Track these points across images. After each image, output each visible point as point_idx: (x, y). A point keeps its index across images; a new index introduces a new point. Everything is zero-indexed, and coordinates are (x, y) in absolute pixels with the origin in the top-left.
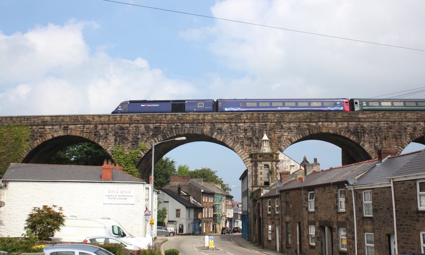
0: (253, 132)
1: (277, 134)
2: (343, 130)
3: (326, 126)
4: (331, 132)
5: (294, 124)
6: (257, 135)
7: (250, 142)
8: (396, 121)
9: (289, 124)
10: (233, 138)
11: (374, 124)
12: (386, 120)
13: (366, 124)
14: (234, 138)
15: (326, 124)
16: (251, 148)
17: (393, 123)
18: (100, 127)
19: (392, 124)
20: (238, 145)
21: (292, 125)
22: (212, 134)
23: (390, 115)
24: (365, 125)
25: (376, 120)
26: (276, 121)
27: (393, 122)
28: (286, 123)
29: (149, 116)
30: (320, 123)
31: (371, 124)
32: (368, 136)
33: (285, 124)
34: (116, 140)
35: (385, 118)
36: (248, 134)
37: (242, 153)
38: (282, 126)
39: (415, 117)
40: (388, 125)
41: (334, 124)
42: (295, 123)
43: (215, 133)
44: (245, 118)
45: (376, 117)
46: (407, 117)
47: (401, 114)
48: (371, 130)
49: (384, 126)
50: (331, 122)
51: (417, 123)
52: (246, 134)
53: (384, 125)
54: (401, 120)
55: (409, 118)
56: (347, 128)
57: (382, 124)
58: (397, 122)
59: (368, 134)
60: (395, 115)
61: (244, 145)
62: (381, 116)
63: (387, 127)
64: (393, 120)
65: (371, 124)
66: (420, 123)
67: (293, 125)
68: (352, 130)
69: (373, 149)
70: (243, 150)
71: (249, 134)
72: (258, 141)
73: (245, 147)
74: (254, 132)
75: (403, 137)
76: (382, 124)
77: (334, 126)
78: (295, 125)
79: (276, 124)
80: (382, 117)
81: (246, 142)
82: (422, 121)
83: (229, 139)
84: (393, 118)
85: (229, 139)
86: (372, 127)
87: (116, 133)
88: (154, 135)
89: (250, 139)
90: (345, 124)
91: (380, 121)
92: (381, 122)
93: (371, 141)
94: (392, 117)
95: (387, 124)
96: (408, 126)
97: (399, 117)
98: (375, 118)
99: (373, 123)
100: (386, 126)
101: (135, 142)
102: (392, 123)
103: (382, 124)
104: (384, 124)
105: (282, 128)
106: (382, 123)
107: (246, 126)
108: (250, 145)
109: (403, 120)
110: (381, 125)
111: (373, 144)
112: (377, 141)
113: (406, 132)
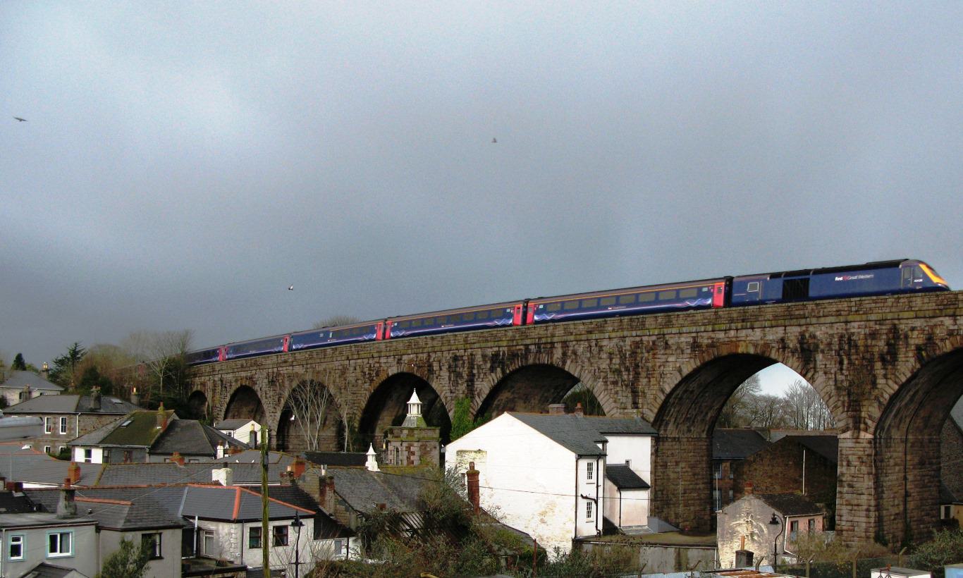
0: (621, 357)
1: (660, 360)
2: (773, 347)
3: (743, 339)
4: (752, 351)
5: (687, 338)
6: (628, 364)
7: (616, 376)
8: (886, 320)
9: (679, 338)
10: (593, 371)
11: (839, 328)
12: (864, 317)
13: (821, 330)
14: (595, 370)
15: (743, 333)
16: (618, 389)
17: (880, 324)
18: (433, 355)
19: (878, 327)
20: (599, 384)
21: (683, 339)
22: (564, 363)
23: (873, 305)
24: (818, 333)
25: (842, 319)
26: (656, 332)
27: (878, 323)
28: (673, 336)
29: (486, 335)
30: (732, 333)
31: (832, 327)
32: (823, 357)
33: (671, 338)
34: (450, 379)
35: (861, 312)
36: (614, 361)
37: (605, 400)
38: (666, 343)
39: (930, 308)
40: (867, 331)
41: (758, 333)
42: (688, 335)
43: (569, 362)
44: (610, 329)
45: (842, 312)
46: (913, 309)
47: (898, 302)
48: (830, 344)
49: (859, 333)
50: (752, 328)
51: (934, 321)
52: (611, 359)
53: (860, 330)
54: (896, 317)
55: (917, 309)
56: (782, 340)
57: (854, 328)
58: (887, 322)
59: (823, 352)
60: (886, 304)
61: (609, 383)
62: (853, 309)
63: (865, 334)
64: (879, 317)
65: (832, 327)
66: (942, 321)
67: (685, 340)
68: (791, 346)
69: (833, 387)
70: (606, 393)
71: (616, 361)
72: (629, 374)
73: (610, 387)
74: (623, 357)
75: (901, 357)
76: (855, 328)
77: (759, 338)
78: (688, 340)
79: (658, 339)
80: (856, 311)
81: (611, 377)
82: (950, 316)
83: (587, 371)
84: (880, 311)
85: (587, 371)
86: (832, 335)
87: (450, 367)
88: (492, 369)
89: (618, 372)
90: (780, 330)
91: (851, 322)
92: (853, 324)
93: (827, 370)
94: (877, 311)
95: (866, 327)
96: (913, 329)
97: (893, 310)
98: (840, 315)
99: (836, 325)
100: (863, 333)
101: (471, 380)
102: (876, 324)
103: (854, 328)
104: (859, 328)
105: (667, 346)
106: (856, 324)
107: (612, 345)
108: (615, 383)
109: (900, 317)
110: (852, 331)
111: (833, 376)
112: (841, 369)
113: (907, 345)
